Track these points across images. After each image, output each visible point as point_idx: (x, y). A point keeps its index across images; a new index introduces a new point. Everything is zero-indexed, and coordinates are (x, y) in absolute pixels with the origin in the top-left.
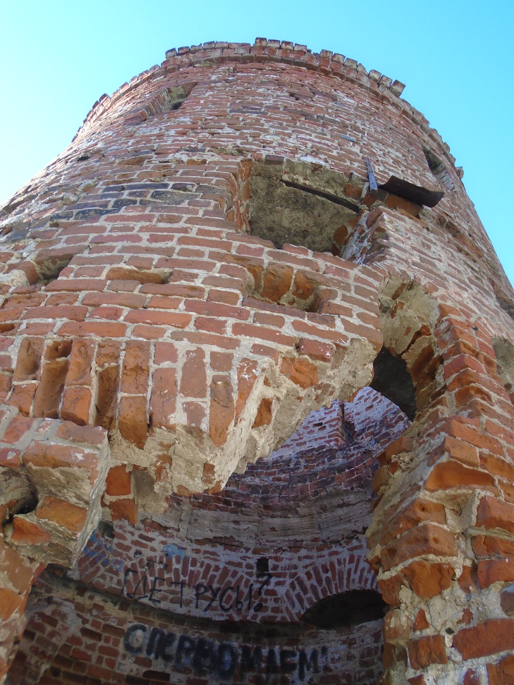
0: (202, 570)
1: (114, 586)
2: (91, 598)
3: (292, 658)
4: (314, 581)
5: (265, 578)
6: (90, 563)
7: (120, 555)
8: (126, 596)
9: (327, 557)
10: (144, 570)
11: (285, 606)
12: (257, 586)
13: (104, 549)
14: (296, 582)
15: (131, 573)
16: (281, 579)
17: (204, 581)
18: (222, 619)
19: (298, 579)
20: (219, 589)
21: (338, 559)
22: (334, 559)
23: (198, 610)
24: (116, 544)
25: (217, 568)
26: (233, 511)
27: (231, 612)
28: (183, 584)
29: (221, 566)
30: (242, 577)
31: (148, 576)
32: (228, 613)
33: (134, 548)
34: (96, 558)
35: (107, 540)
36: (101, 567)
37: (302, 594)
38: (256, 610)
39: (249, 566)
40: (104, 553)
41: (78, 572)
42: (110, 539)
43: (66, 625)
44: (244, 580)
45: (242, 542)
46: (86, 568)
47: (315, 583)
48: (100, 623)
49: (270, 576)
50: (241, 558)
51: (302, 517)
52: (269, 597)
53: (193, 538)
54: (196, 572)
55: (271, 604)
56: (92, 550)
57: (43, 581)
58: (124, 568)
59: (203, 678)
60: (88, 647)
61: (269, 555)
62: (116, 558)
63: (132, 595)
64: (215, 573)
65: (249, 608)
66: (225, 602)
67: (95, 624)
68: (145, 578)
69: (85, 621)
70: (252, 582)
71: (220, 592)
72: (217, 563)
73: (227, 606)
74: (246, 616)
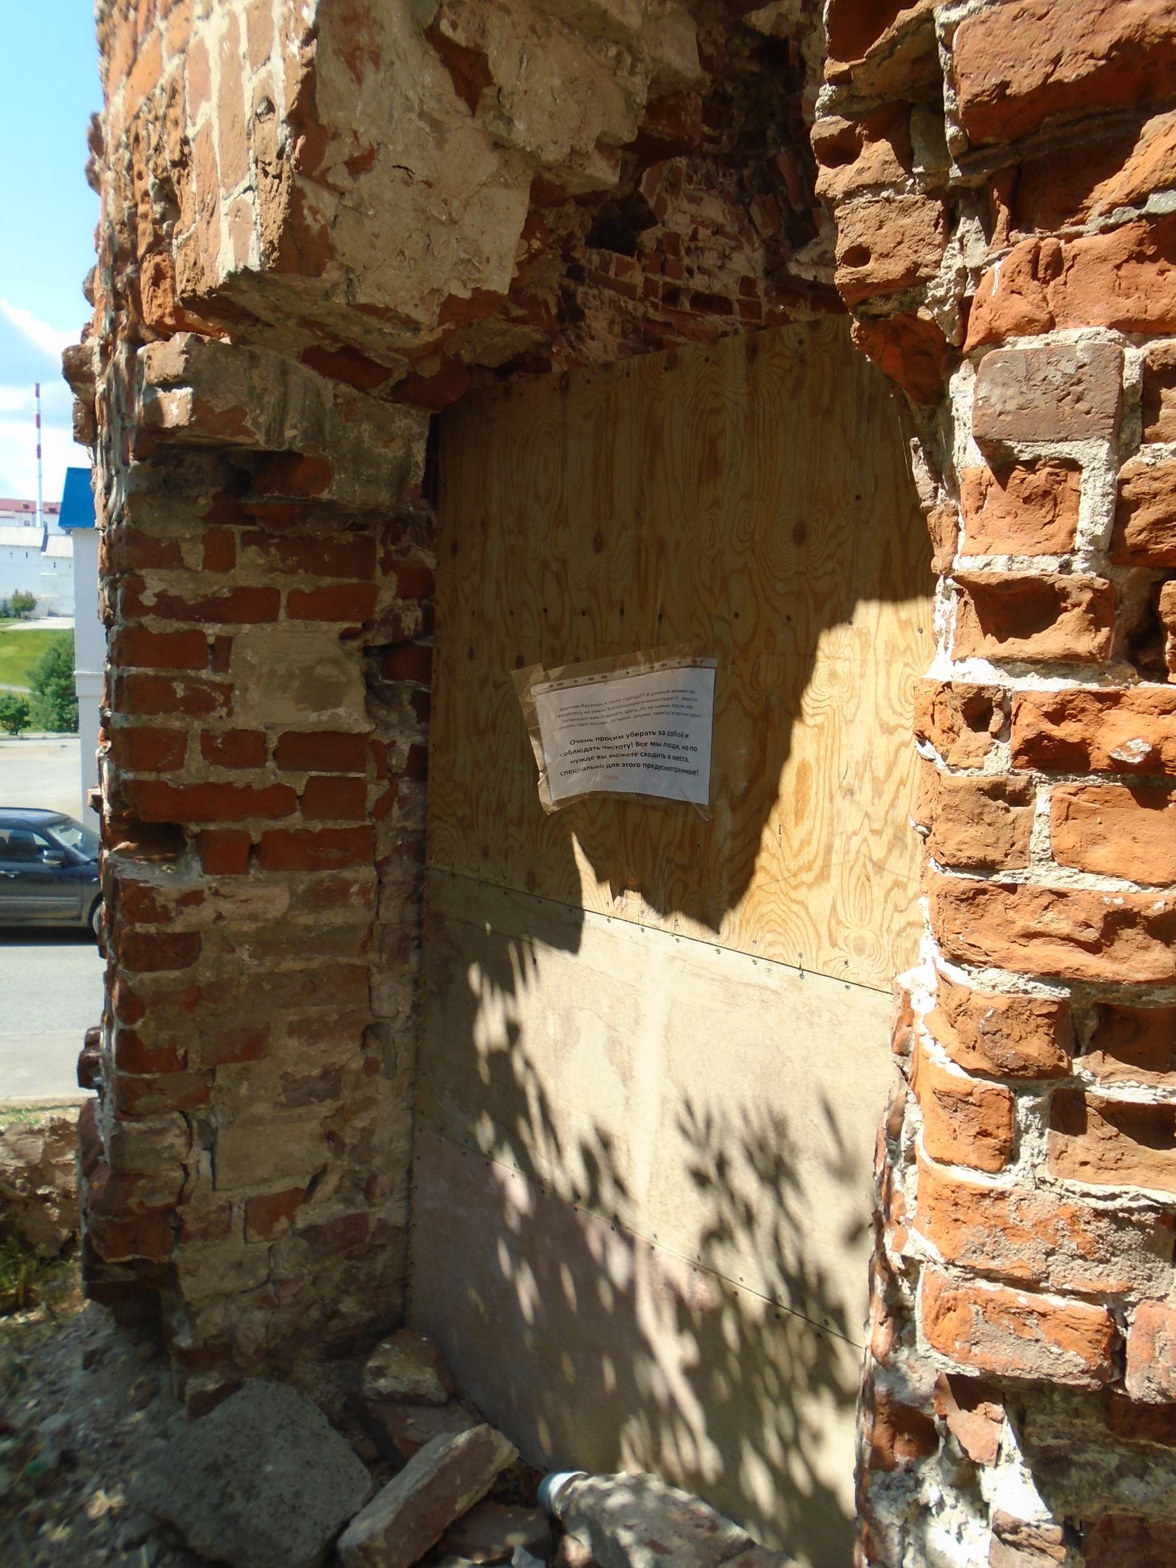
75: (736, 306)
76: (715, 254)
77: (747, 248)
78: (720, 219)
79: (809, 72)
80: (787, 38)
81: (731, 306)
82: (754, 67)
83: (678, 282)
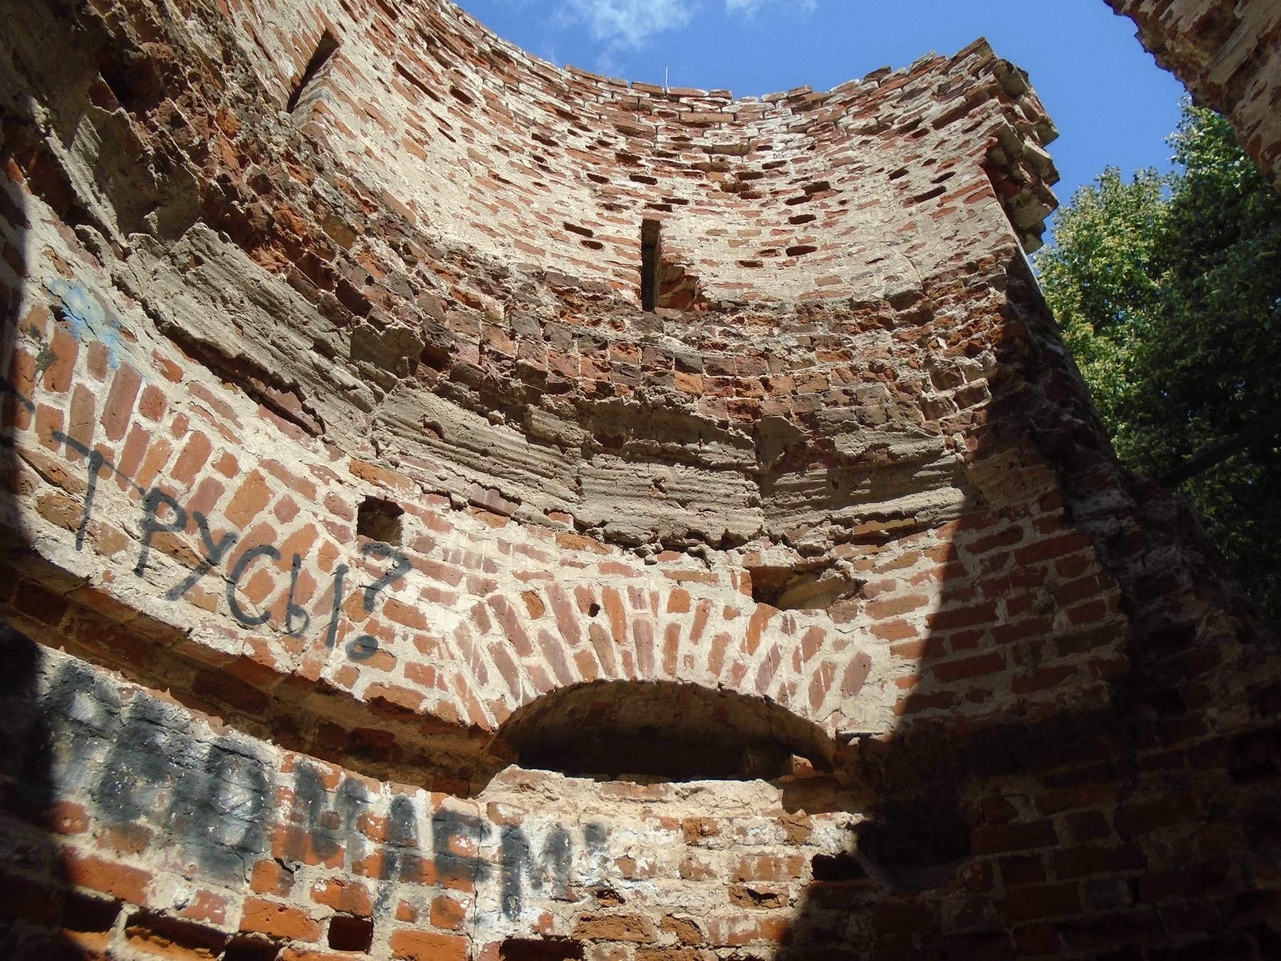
0: (179, 445)
3: (475, 841)
4: (549, 624)
5: (387, 564)
9: (593, 571)
11: (455, 670)
12: (358, 579)
14: (490, 611)
16: (442, 586)
17: (177, 485)
18: (231, 648)
19: (498, 603)
20: (229, 538)
21: (631, 589)
22: (620, 584)
23: (141, 585)
25: (229, 466)
26: (327, 311)
27: (263, 632)
28: (99, 462)
29: (247, 464)
30: (309, 534)
32: (256, 636)
37: (510, 650)
38: (353, 656)
39: (334, 505)
44: (318, 544)
45: (320, 421)
47: (556, 633)
49: (405, 562)
50: (312, 468)
51: (534, 437)
52: (398, 627)
53: (167, 316)
54: (153, 441)
55: (404, 649)
59: (133, 861)
61: (406, 500)
64: (219, 477)
65: (329, 641)
66: (246, 592)
70: (343, 559)
71: (232, 549)
72: (231, 448)
73: (253, 611)
74: (320, 665)
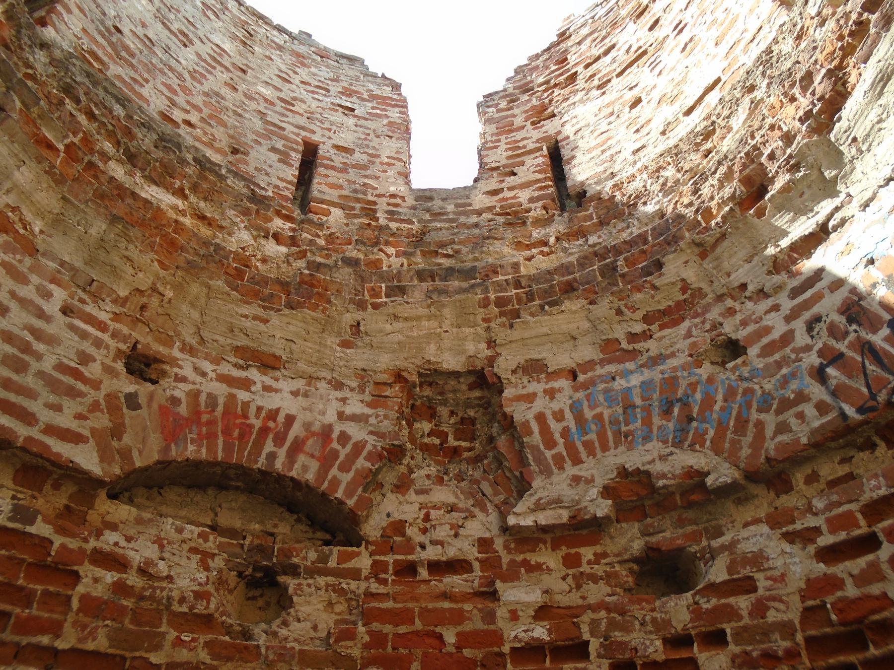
1: (816, 424)
2: (813, 478)
6: (735, 432)
7: (779, 365)
8: (858, 417)
10: (852, 337)
13: (745, 385)
15: (830, 371)
24: (759, 356)
31: (871, 337)
33: (799, 325)
34: (739, 413)
35: (736, 368)
36: (762, 416)
40: (748, 392)
41: (727, 465)
42: (739, 361)
43: (777, 573)
46: (735, 444)
48: (850, 513)
56: (722, 409)
57: (690, 529)
58: (810, 375)
60: (861, 579)
62: (778, 376)
63: (871, 403)
67: (847, 521)
68: (868, 349)
69: (807, 536)
75: (476, 565)
76: (448, 527)
77: (481, 516)
78: (451, 499)
79: (505, 381)
80: (483, 369)
81: (470, 565)
82: (477, 393)
83: (410, 557)
